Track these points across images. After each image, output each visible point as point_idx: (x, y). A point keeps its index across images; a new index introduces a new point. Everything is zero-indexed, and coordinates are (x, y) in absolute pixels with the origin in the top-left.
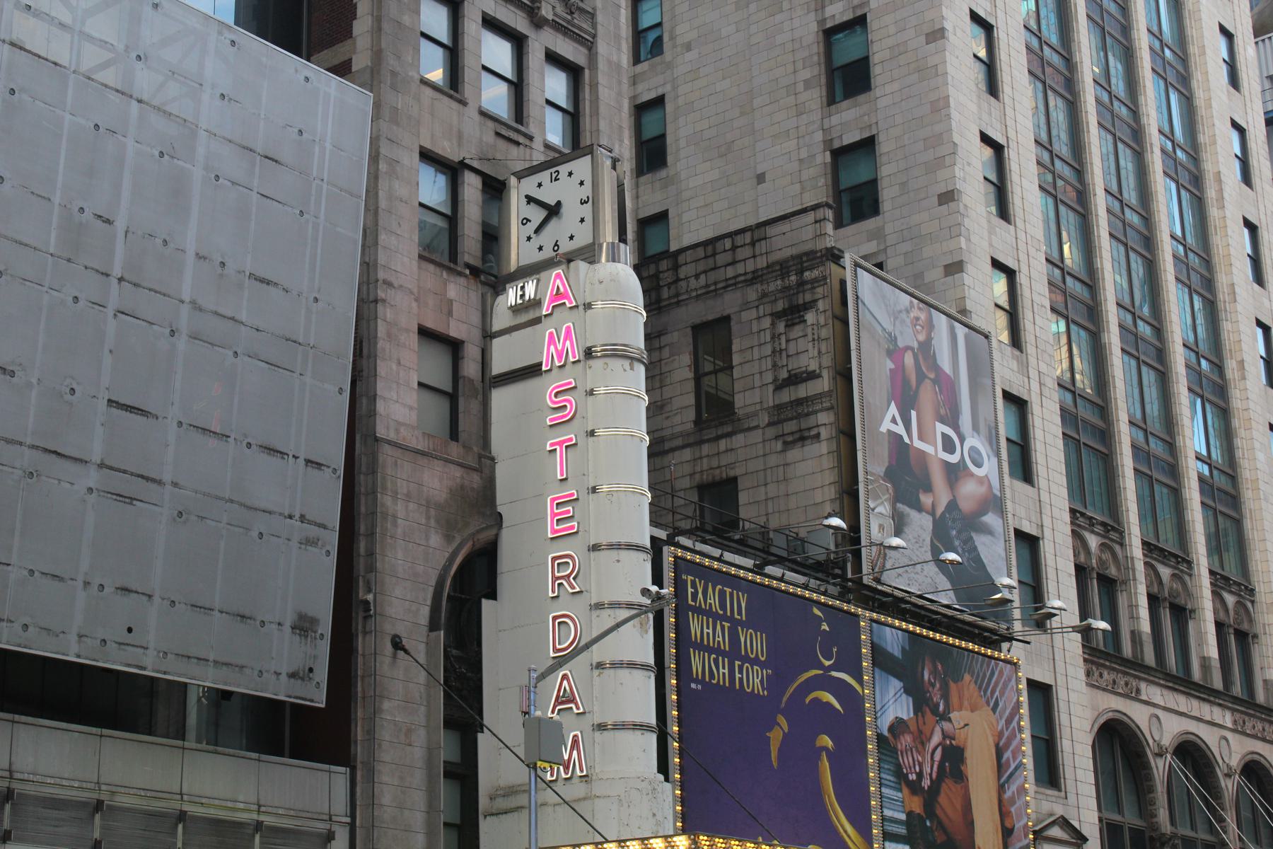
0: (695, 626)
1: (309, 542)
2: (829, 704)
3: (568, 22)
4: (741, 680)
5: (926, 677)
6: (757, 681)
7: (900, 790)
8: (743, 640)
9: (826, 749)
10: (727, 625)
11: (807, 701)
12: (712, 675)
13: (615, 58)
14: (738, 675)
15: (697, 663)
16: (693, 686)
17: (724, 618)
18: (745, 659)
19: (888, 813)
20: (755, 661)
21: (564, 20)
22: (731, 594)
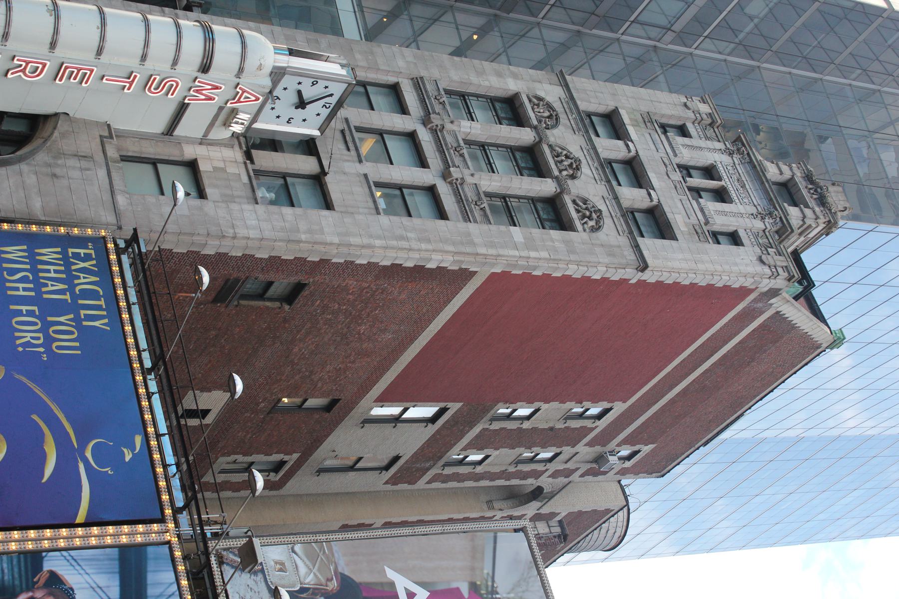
0: (49, 254)
2: (43, 458)
3: (467, 200)
4: (19, 313)
8: (62, 319)
10: (68, 297)
11: (35, 417)
13: (477, 240)
14: (24, 308)
15: (15, 252)
17: (74, 297)
18: (46, 326)
20: (49, 340)
21: (466, 196)
22: (99, 308)
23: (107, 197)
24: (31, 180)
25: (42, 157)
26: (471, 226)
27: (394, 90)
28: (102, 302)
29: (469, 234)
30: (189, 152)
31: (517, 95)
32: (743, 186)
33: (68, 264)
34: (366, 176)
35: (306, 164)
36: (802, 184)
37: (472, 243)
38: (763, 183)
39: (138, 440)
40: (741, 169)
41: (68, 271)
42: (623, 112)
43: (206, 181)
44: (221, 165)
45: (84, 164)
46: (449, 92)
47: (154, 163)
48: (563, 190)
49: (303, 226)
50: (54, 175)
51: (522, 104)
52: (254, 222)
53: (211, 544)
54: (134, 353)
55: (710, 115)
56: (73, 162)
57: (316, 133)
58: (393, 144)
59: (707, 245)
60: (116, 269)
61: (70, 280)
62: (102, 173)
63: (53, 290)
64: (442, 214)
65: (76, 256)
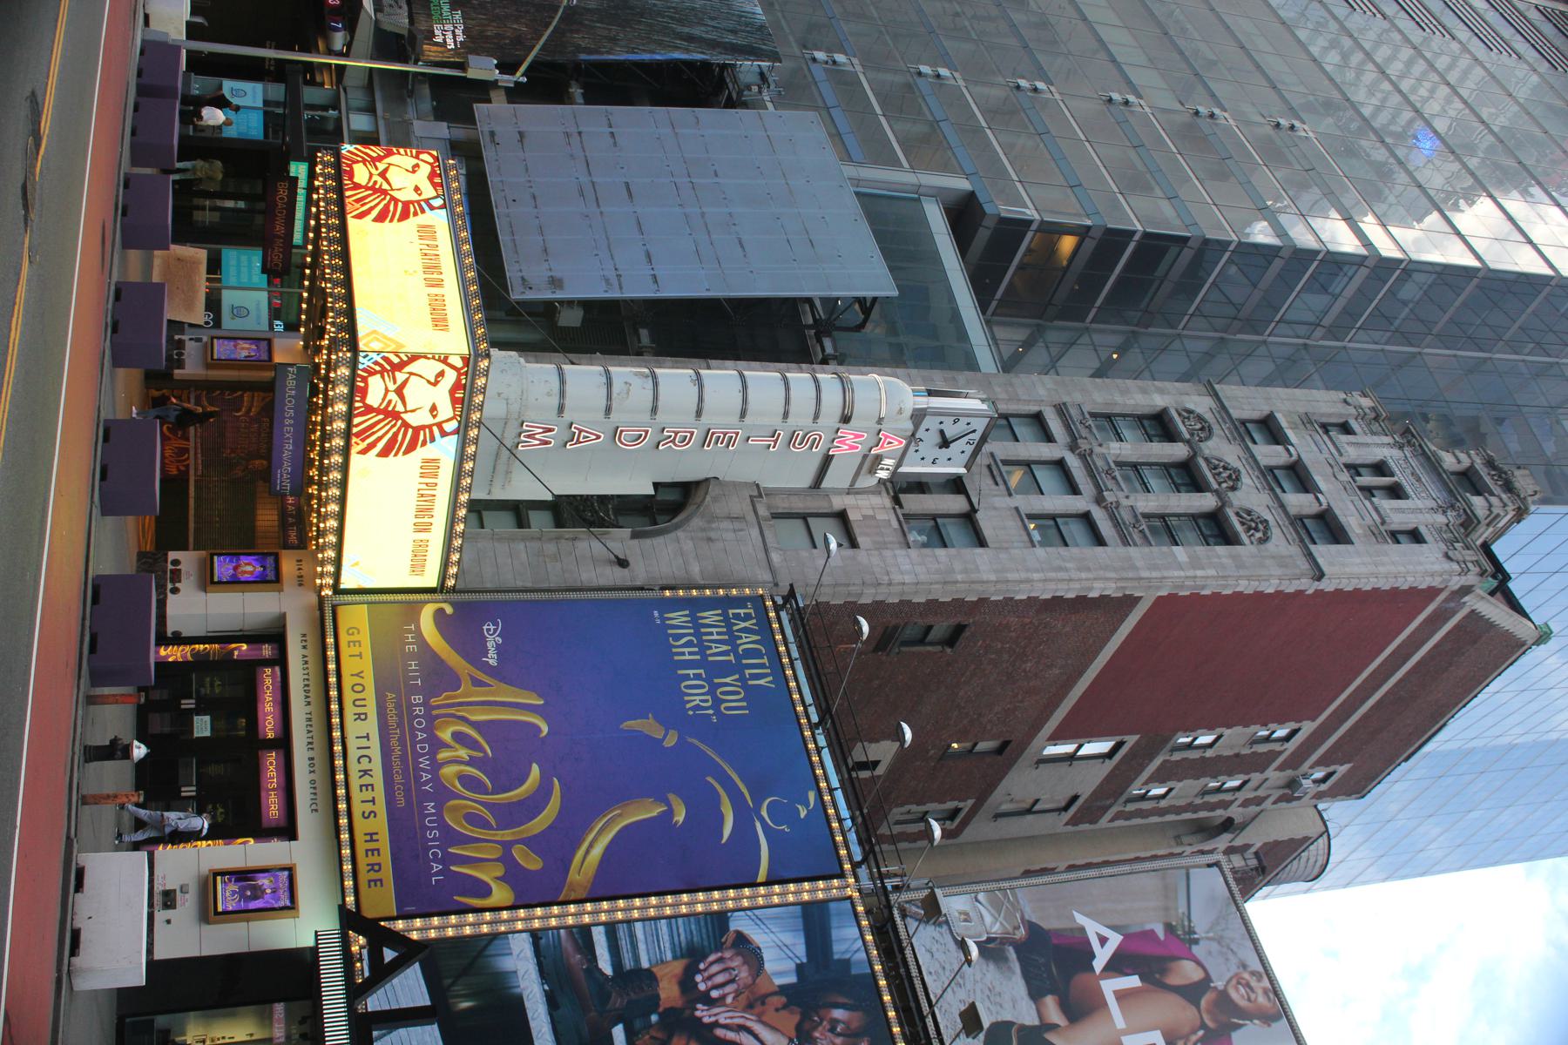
0: (710, 616)
1: (607, 281)
4: (687, 677)
5: (838, 1014)
6: (697, 700)
7: (675, 958)
8: (728, 680)
9: (670, 813)
10: (732, 658)
11: (710, 779)
12: (678, 637)
13: (1139, 564)
14: (691, 672)
15: (678, 618)
16: (656, 614)
19: (638, 925)
20: (717, 702)
22: (762, 666)
23: (762, 555)
24: (688, 546)
25: (696, 522)
26: (1132, 550)
27: (1038, 419)
28: (765, 660)
29: (1130, 559)
30: (838, 503)
31: (1165, 411)
32: (1419, 480)
33: (729, 625)
34: (1017, 509)
35: (956, 504)
36: (1483, 471)
37: (1134, 568)
38: (1439, 475)
39: (812, 796)
40: (1414, 462)
41: (730, 632)
42: (1279, 416)
43: (857, 531)
44: (870, 513)
45: (737, 525)
46: (1094, 415)
47: (804, 517)
48: (1224, 502)
49: (958, 566)
50: (710, 539)
51: (1171, 419)
52: (907, 567)
53: (893, 897)
54: (800, 709)
55: (1373, 409)
56: (726, 524)
57: (963, 471)
58: (1043, 475)
59: (1386, 547)
60: (776, 626)
61: (732, 640)
62: (755, 532)
63: (718, 651)
64: (1099, 541)
65: (737, 616)
